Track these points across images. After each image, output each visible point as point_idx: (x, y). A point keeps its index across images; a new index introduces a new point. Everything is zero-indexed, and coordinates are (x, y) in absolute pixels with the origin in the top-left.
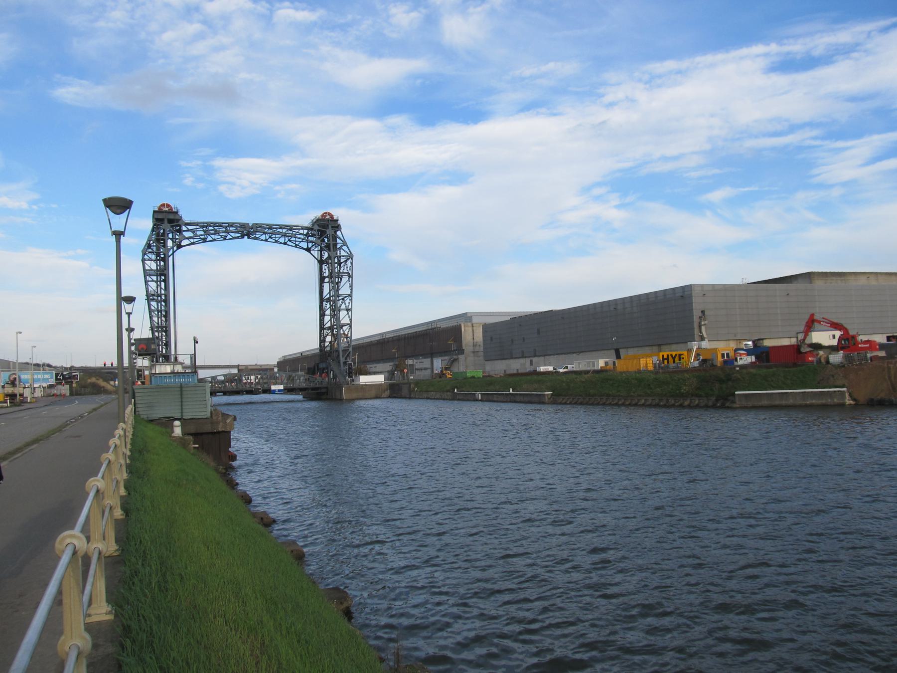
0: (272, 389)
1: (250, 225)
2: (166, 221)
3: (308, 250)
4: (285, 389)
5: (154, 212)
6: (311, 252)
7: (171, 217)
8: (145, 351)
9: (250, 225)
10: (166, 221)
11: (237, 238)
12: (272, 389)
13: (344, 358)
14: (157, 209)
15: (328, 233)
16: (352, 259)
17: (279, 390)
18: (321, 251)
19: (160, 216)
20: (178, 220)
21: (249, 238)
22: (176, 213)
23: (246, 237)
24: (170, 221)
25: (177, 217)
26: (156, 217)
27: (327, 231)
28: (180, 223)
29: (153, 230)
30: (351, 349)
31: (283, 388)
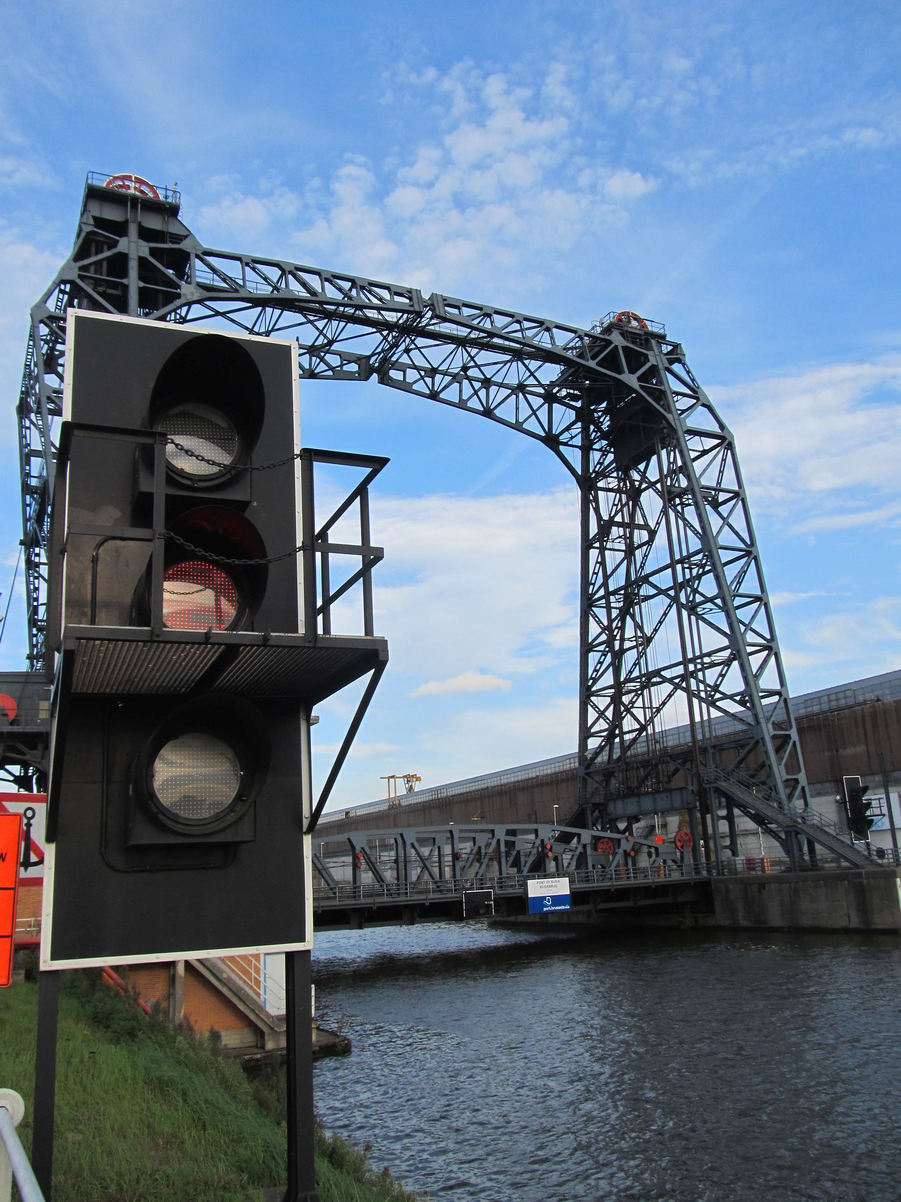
0: (530, 896)
1: (426, 296)
2: (133, 230)
3: (552, 441)
4: (576, 897)
5: (94, 194)
6: (562, 448)
7: (154, 223)
8: (12, 723)
9: (426, 296)
10: (133, 230)
11: (349, 376)
12: (531, 895)
13: (782, 767)
14: (102, 183)
15: (652, 361)
16: (730, 446)
17: (557, 900)
18: (586, 449)
19: (113, 214)
20: (178, 238)
21: (385, 380)
22: (172, 211)
23: (375, 376)
24: (146, 234)
25: (173, 229)
26: (97, 214)
27: (650, 353)
28: (184, 245)
29: (79, 256)
30: (794, 734)
31: (567, 892)
